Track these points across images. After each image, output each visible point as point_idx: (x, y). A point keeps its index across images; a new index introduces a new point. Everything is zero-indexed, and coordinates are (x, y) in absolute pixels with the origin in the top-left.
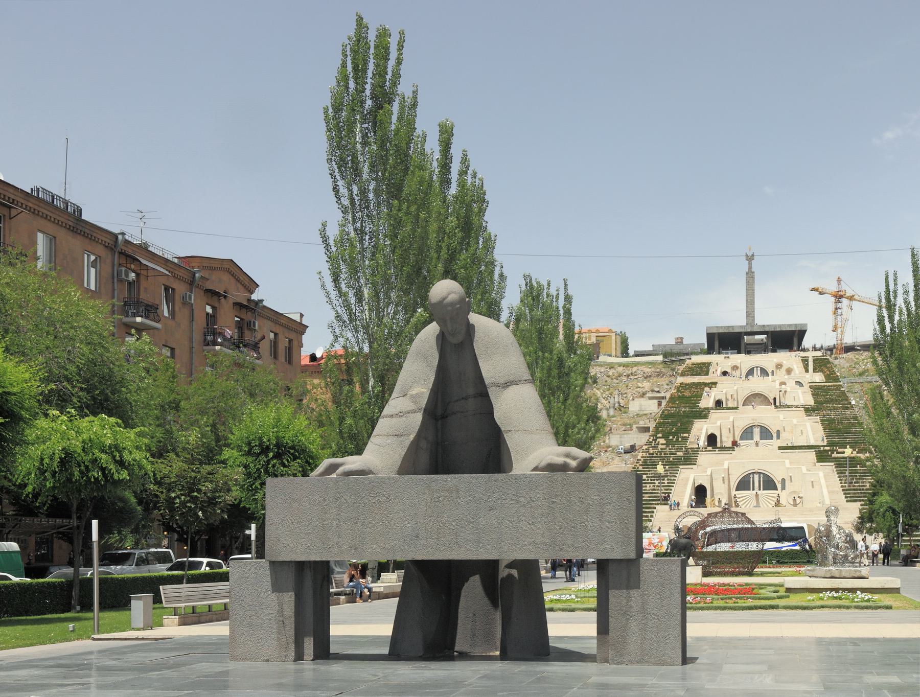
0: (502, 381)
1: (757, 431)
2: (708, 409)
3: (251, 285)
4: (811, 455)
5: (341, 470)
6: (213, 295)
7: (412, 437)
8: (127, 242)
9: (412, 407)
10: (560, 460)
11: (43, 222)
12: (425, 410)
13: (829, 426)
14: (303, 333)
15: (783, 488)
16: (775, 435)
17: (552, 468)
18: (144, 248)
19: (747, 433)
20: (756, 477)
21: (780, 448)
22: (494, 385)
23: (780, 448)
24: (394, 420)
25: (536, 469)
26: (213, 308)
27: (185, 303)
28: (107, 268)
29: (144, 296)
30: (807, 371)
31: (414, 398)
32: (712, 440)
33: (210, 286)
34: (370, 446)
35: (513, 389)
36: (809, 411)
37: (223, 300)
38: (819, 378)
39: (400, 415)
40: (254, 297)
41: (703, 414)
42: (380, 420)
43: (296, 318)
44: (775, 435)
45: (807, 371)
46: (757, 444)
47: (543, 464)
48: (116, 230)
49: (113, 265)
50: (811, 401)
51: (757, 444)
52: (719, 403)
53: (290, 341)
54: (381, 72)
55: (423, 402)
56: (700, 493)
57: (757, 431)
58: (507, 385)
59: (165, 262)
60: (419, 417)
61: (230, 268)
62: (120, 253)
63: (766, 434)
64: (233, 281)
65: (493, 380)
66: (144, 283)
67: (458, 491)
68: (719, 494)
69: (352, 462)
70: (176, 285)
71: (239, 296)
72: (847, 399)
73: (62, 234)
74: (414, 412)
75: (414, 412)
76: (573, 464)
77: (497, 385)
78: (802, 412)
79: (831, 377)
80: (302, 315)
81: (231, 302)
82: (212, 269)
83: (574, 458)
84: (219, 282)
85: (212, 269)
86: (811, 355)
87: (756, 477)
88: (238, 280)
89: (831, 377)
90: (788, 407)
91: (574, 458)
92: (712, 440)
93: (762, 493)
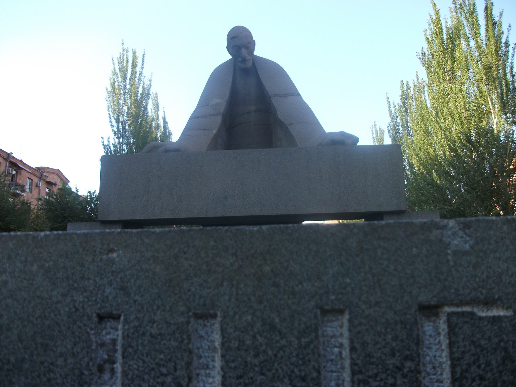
6: (50, 184)
8: (13, 157)
26: (50, 190)
27: (37, 186)
29: (19, 181)
33: (48, 180)
48: (9, 152)
49: (6, 166)
54: (133, 73)
59: (30, 168)
61: (58, 173)
64: (59, 179)
66: (19, 176)
70: (33, 178)
82: (50, 173)
84: (52, 178)
85: (50, 173)
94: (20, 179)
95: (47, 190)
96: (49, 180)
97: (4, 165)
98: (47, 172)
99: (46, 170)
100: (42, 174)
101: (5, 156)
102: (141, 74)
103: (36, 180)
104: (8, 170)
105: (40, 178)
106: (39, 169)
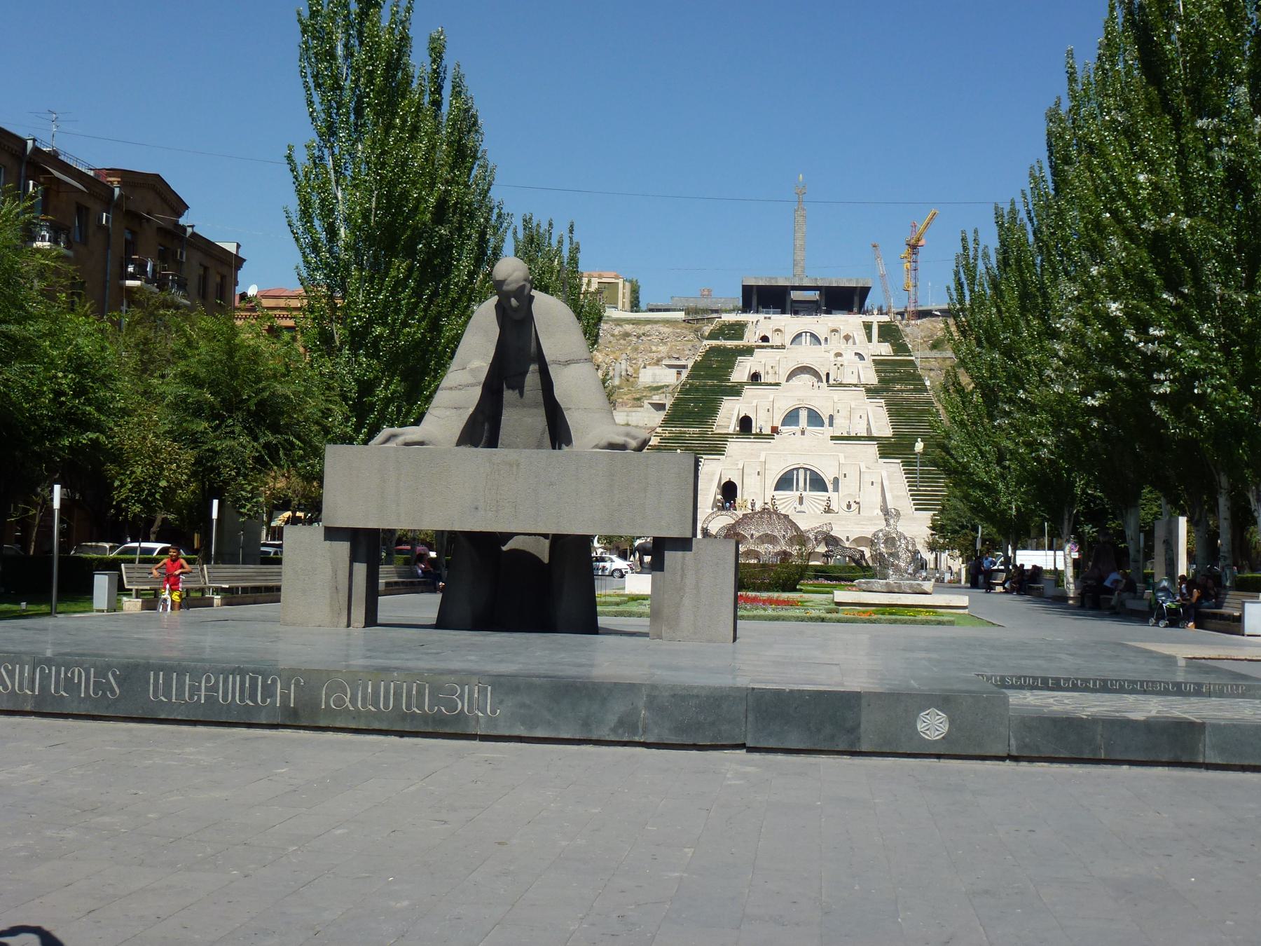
0: (563, 359)
1: (803, 415)
2: (742, 385)
3: (179, 207)
4: (873, 449)
5: (401, 439)
7: (471, 410)
9: (471, 380)
10: (619, 439)
13: (897, 411)
14: (239, 267)
15: (836, 489)
16: (826, 421)
17: (612, 446)
19: (791, 418)
20: (801, 472)
21: (833, 438)
22: (555, 362)
23: (833, 438)
24: (454, 393)
25: (596, 446)
26: (133, 233)
30: (870, 340)
31: (472, 370)
32: (745, 424)
34: (427, 418)
35: (574, 368)
36: (872, 392)
38: (885, 349)
39: (459, 387)
40: (182, 221)
41: (736, 391)
42: (439, 393)
43: (231, 248)
44: (826, 421)
45: (870, 340)
46: (803, 433)
47: (604, 442)
50: (872, 378)
51: (803, 433)
52: (755, 378)
53: (223, 277)
55: (482, 377)
56: (729, 491)
57: (803, 415)
58: (568, 363)
60: (478, 391)
62: (28, 163)
63: (815, 418)
65: (553, 358)
67: (518, 465)
68: (754, 493)
69: (411, 433)
71: (160, 218)
72: (920, 378)
74: (473, 385)
75: (473, 385)
76: (634, 443)
77: (559, 363)
78: (862, 393)
79: (900, 348)
80: (238, 246)
83: (634, 438)
86: (876, 319)
87: (801, 472)
88: (164, 200)
89: (900, 348)
90: (845, 385)
91: (634, 438)
92: (745, 424)
93: (809, 495)
95: (129, 237)
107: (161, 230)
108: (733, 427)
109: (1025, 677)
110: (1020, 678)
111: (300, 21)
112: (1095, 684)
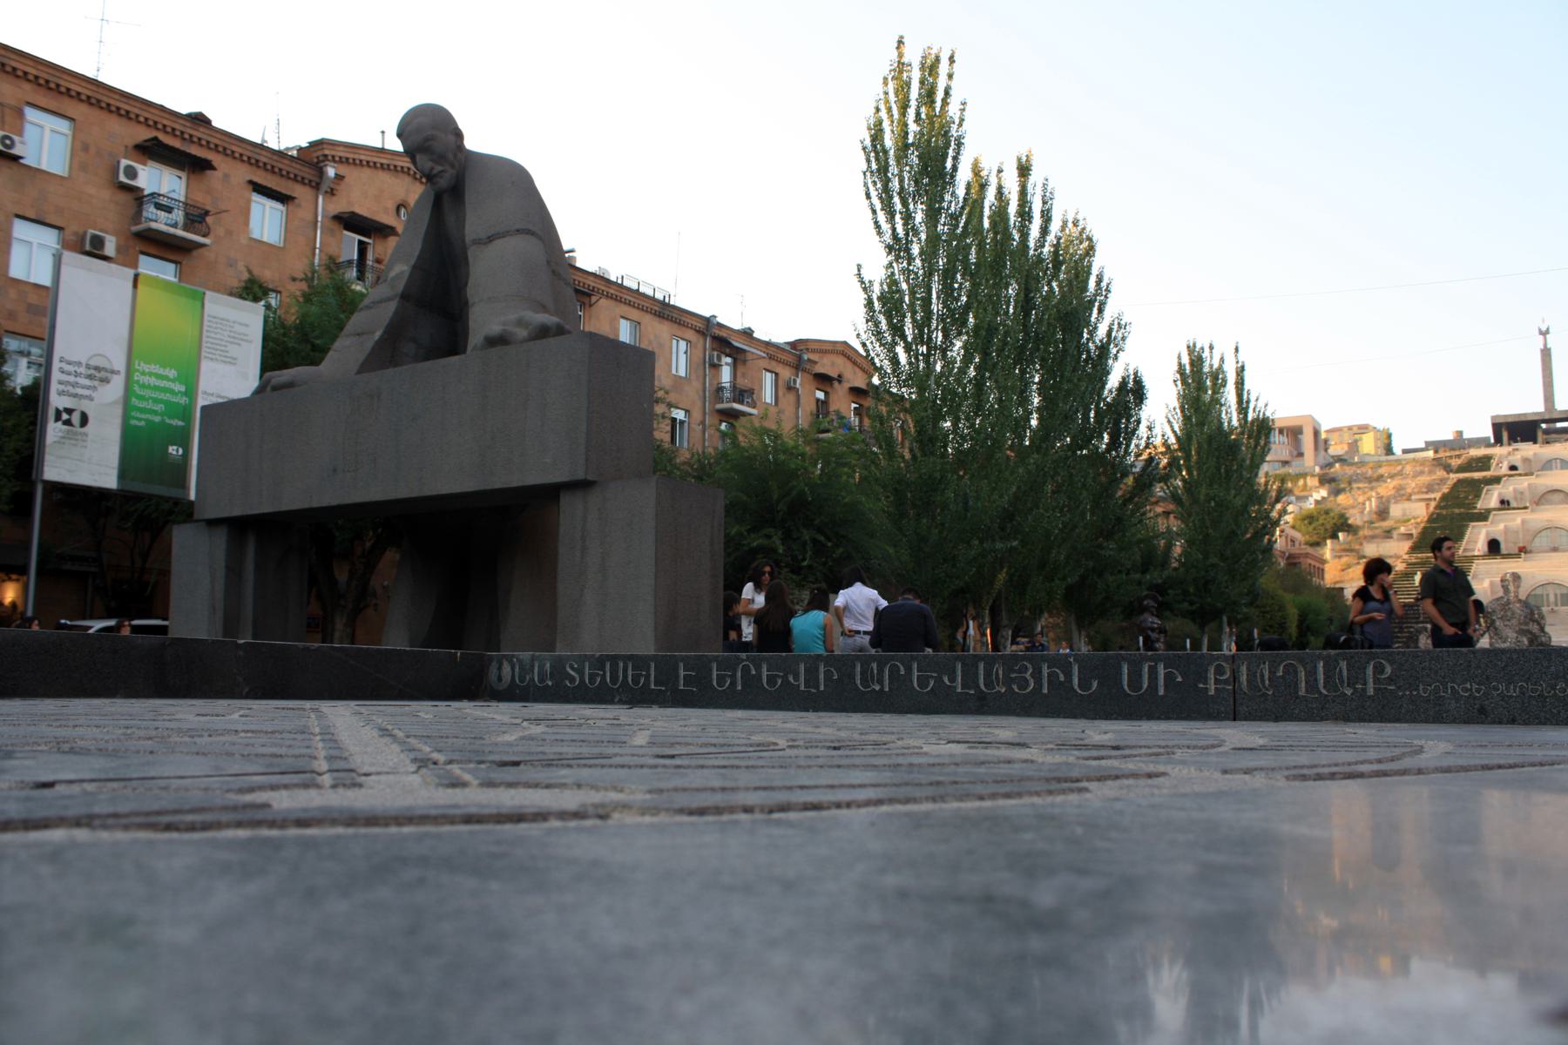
6: (824, 380)
7: (378, 335)
8: (720, 325)
10: (495, 329)
11: (624, 309)
12: (404, 297)
18: (747, 333)
22: (478, 242)
26: (826, 393)
27: (790, 388)
28: (698, 353)
33: (819, 369)
35: (499, 243)
37: (836, 384)
48: (707, 315)
55: (400, 287)
58: (491, 239)
60: (392, 306)
64: (849, 365)
71: (860, 383)
73: (647, 320)
74: (390, 299)
75: (390, 299)
76: (522, 333)
81: (847, 385)
84: (826, 366)
85: (824, 352)
94: (744, 375)
96: (822, 370)
97: (700, 345)
98: (814, 351)
99: (812, 346)
100: (800, 357)
101: (699, 325)
102: (947, 93)
103: (786, 373)
104: (711, 357)
105: (798, 366)
106: (794, 345)
107: (856, 392)
108: (1481, 546)
109: (614, 659)
110: (600, 662)
111: (864, 149)
112: (812, 679)
